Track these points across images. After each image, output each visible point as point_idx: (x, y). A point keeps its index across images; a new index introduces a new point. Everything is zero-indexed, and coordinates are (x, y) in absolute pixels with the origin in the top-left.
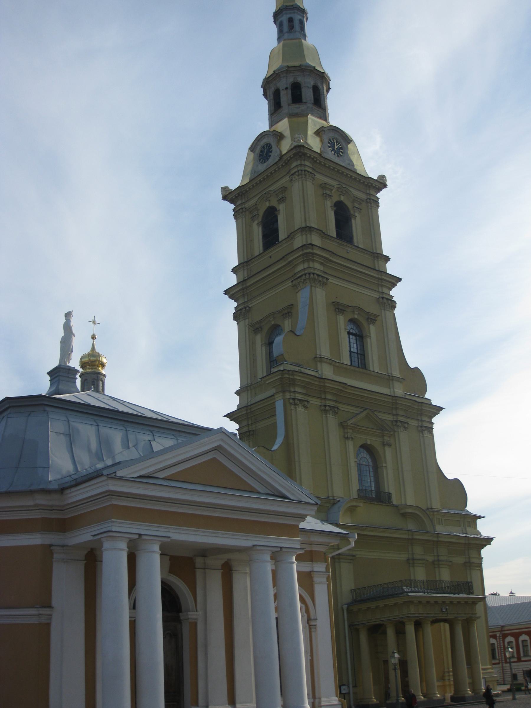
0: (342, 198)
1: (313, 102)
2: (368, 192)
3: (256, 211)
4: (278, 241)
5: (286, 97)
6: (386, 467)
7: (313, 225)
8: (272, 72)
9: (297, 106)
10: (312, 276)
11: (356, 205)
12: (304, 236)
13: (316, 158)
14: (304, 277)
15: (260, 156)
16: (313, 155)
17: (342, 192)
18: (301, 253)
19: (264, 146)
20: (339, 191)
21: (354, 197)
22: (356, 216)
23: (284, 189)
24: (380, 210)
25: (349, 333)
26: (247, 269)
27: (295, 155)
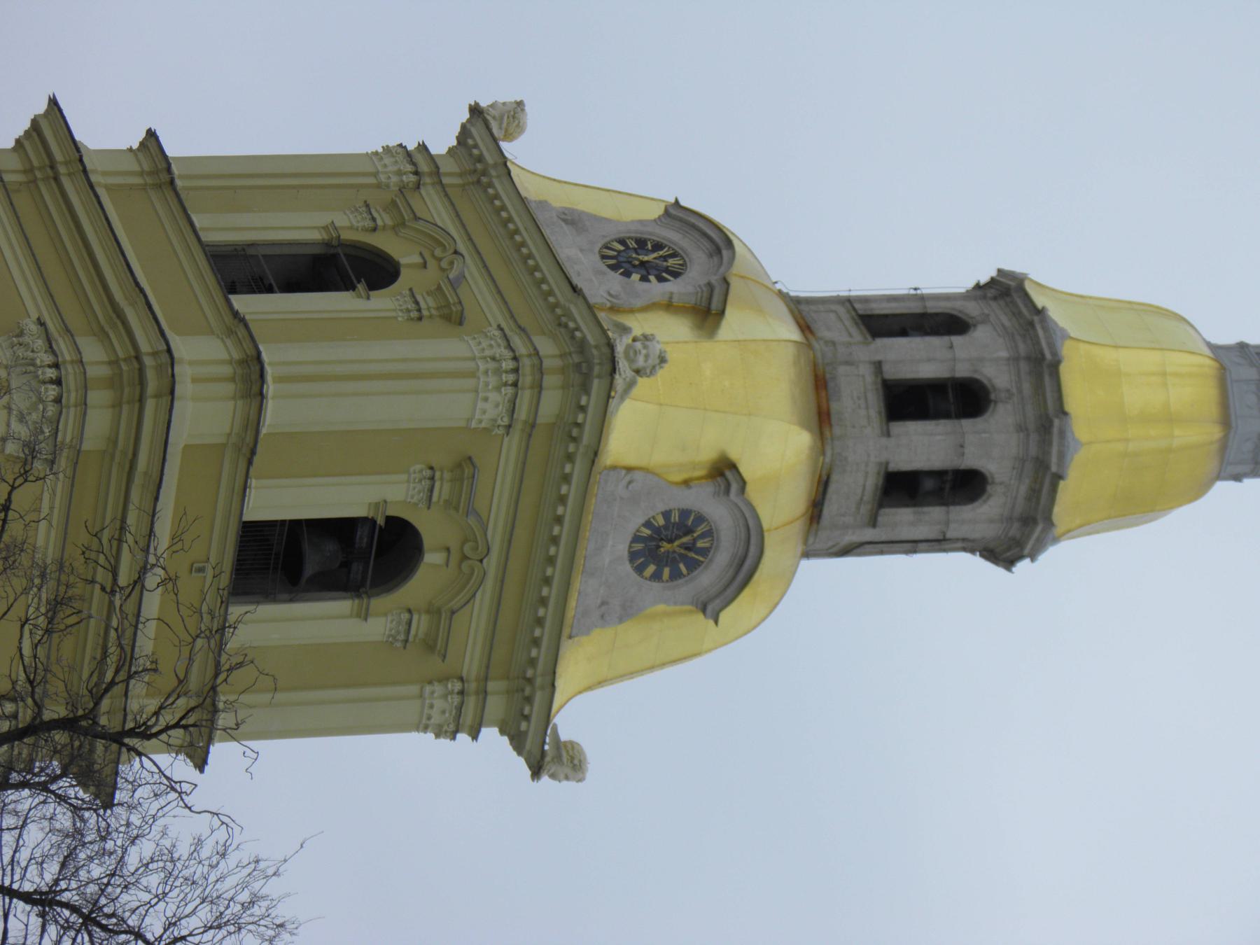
0: (432, 558)
2: (491, 686)
3: (389, 222)
4: (232, 288)
7: (270, 406)
8: (1040, 301)
11: (421, 624)
12: (227, 370)
14: (48, 359)
15: (641, 243)
16: (589, 420)
18: (145, 347)
19: (681, 256)
21: (453, 613)
22: (366, 619)
23: (453, 317)
24: (421, 743)
26: (144, 187)
27: (582, 346)
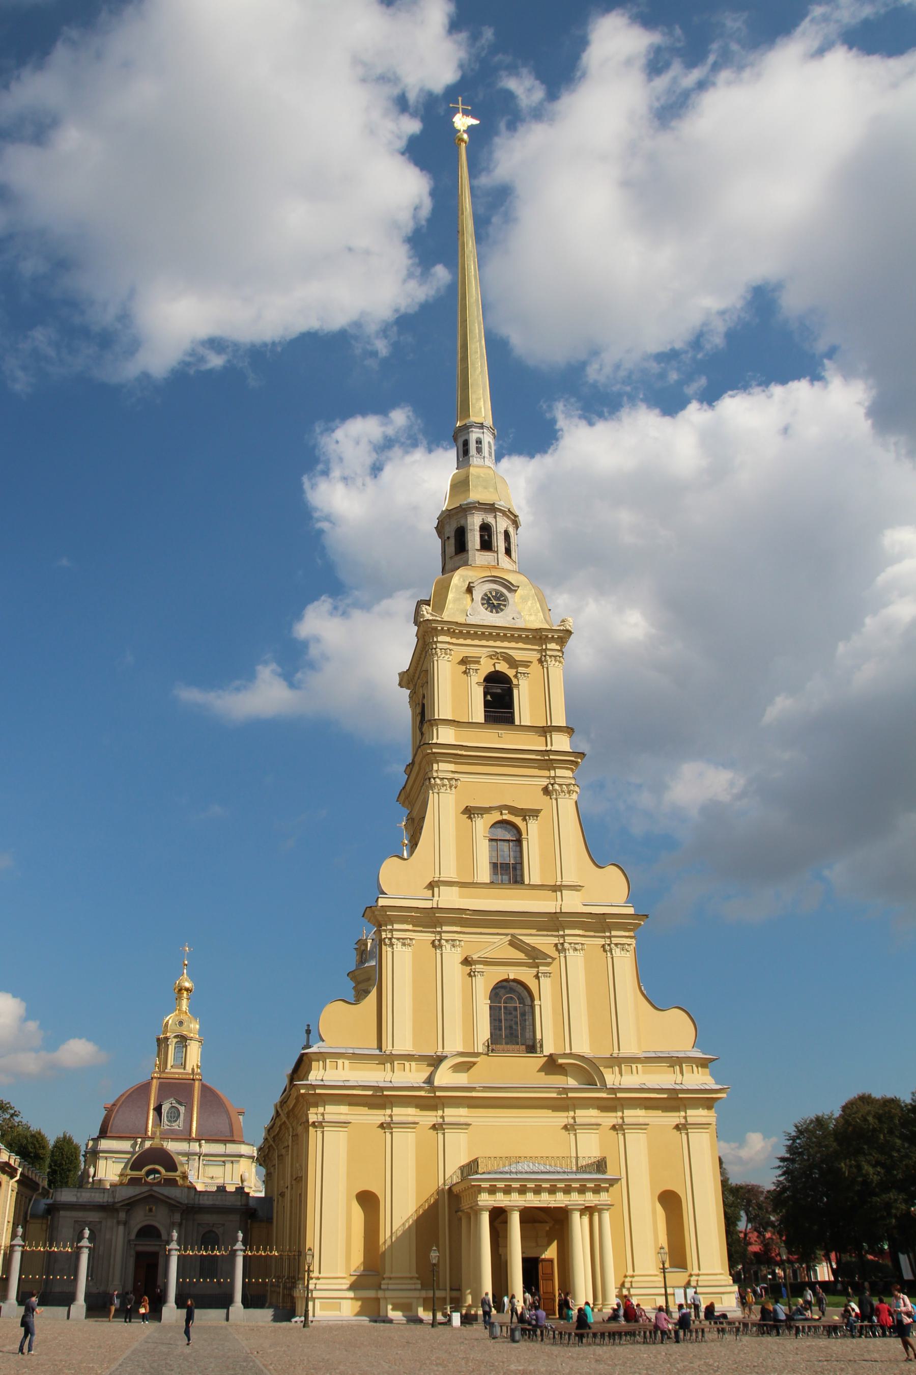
0: (497, 669)
1: (479, 547)
5: (451, 549)
6: (540, 1006)
9: (459, 557)
10: (432, 780)
13: (452, 628)
17: (498, 659)
20: (492, 659)
25: (491, 840)
